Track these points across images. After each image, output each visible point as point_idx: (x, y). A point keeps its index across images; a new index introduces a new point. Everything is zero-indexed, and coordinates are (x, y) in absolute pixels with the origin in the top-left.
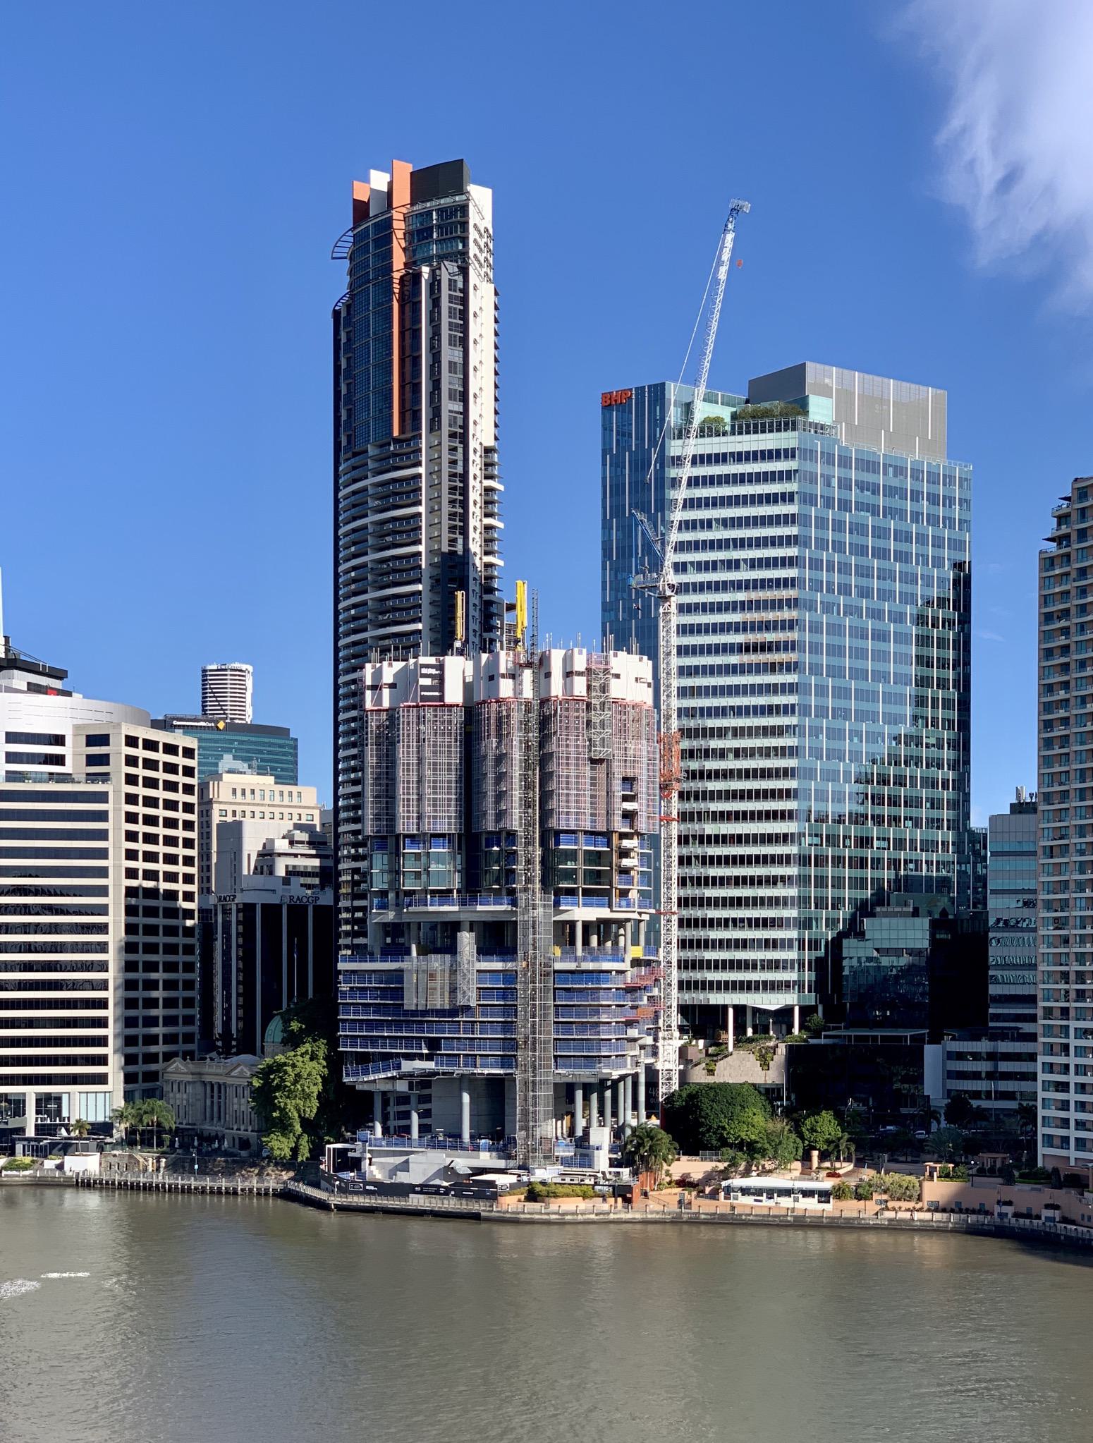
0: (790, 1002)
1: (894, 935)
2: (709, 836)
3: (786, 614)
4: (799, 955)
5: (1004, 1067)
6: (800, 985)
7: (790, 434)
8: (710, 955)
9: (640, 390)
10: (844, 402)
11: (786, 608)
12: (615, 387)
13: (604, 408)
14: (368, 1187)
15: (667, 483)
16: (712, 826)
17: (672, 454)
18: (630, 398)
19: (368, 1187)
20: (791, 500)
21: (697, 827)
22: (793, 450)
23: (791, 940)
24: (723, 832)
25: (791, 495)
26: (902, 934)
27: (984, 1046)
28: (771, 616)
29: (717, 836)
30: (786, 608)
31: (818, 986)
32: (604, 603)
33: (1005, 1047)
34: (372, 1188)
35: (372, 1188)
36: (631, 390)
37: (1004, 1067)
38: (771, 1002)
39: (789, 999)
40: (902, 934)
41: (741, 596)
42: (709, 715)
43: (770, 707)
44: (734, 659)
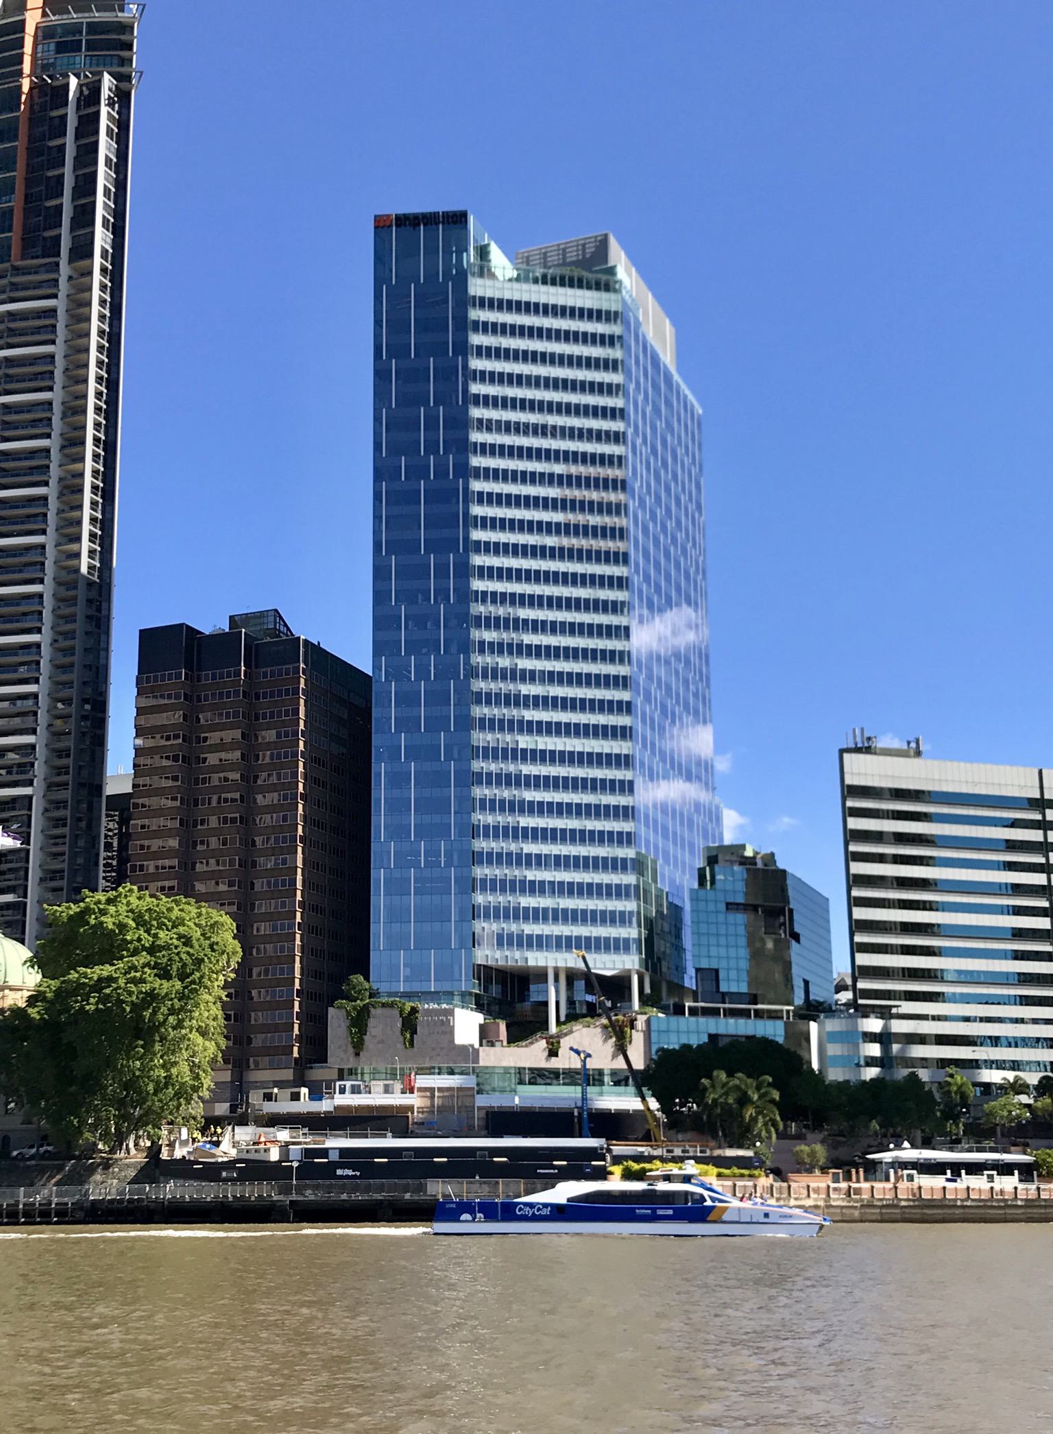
0: (628, 966)
2: (524, 751)
3: (613, 497)
8: (527, 901)
15: (470, 326)
16: (528, 738)
21: (508, 738)
28: (594, 495)
29: (534, 751)
34: (350, 1173)
35: (350, 1173)
38: (606, 965)
41: (559, 468)
42: (522, 604)
43: (596, 601)
44: (551, 541)
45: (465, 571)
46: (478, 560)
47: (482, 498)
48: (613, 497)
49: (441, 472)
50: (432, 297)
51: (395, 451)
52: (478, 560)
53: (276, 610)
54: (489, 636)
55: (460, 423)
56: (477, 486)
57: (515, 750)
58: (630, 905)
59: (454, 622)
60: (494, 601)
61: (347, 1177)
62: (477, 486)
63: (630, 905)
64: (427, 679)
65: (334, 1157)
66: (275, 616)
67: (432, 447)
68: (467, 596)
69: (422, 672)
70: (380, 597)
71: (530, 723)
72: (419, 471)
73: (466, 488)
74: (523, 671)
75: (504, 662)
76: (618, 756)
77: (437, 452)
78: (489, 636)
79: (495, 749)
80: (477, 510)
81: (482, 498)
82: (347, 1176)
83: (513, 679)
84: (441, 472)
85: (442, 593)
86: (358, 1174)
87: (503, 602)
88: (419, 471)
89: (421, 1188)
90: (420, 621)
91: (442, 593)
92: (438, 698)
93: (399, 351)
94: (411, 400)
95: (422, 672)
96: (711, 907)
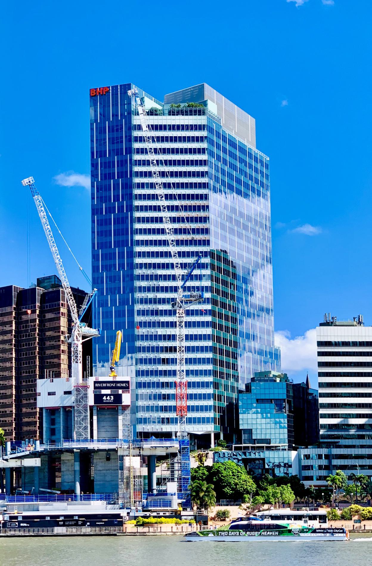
1: (267, 391)
2: (160, 336)
3: (202, 214)
4: (214, 402)
5: (335, 462)
6: (214, 420)
7: (202, 117)
9: (115, 88)
10: (219, 108)
11: (202, 210)
12: (99, 85)
13: (91, 97)
14: (22, 525)
17: (135, 124)
18: (108, 92)
19: (22, 525)
20: (204, 153)
22: (204, 125)
23: (209, 394)
24: (168, 333)
25: (204, 149)
26: (272, 391)
27: (324, 451)
29: (165, 336)
30: (202, 210)
31: (222, 422)
32: (93, 205)
33: (336, 451)
34: (25, 525)
35: (25, 525)
36: (109, 87)
37: (335, 462)
38: (199, 429)
39: (210, 428)
40: (272, 391)
45: (131, 255)
46: (138, 249)
47: (139, 220)
48: (202, 214)
49: (121, 208)
50: (116, 128)
51: (101, 199)
52: (138, 249)
53: (56, 276)
54: (144, 284)
55: (129, 186)
56: (138, 214)
57: (156, 336)
58: (210, 403)
59: (127, 279)
60: (146, 268)
61: (25, 527)
62: (138, 214)
63: (210, 403)
64: (115, 305)
65: (20, 519)
66: (55, 278)
67: (116, 198)
68: (132, 266)
69: (113, 302)
70: (95, 269)
71: (163, 323)
72: (111, 210)
73: (132, 217)
74: (160, 299)
75: (151, 295)
76: (205, 335)
77: (118, 200)
78: (144, 284)
79: (147, 336)
80: (138, 226)
81: (139, 220)
82: (25, 526)
83: (155, 303)
84: (121, 208)
85: (122, 266)
86: (29, 525)
87: (150, 268)
88: (111, 210)
89: (53, 531)
90: (113, 279)
91: (122, 266)
92: (120, 314)
93: (101, 154)
94: (108, 176)
95: (113, 302)
96: (249, 402)
